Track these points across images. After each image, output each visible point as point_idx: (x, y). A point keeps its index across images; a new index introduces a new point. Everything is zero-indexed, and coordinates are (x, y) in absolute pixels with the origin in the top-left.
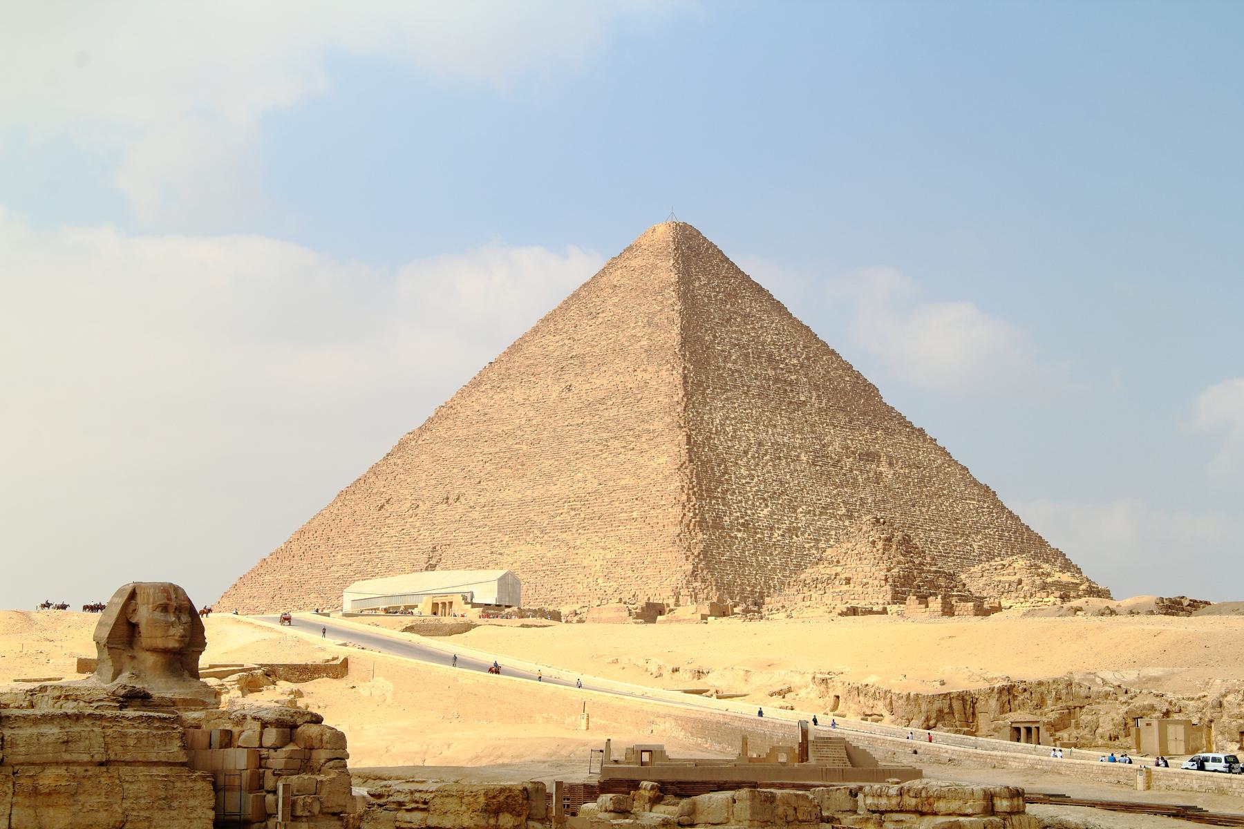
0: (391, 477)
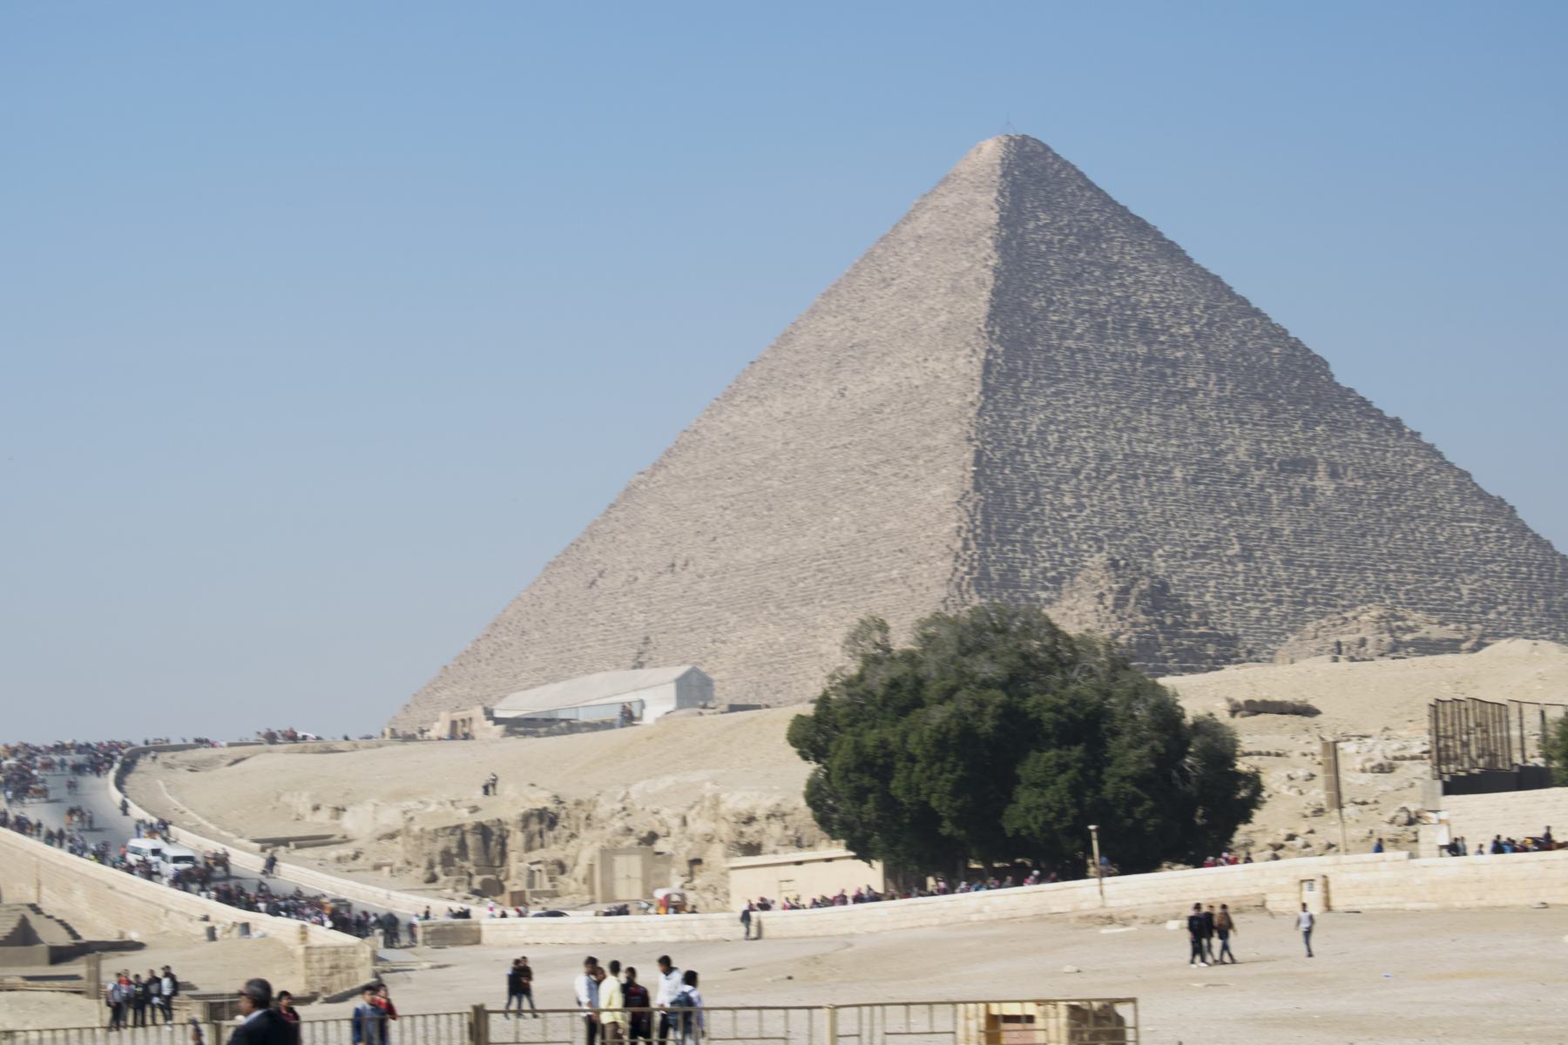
0: (609, 538)
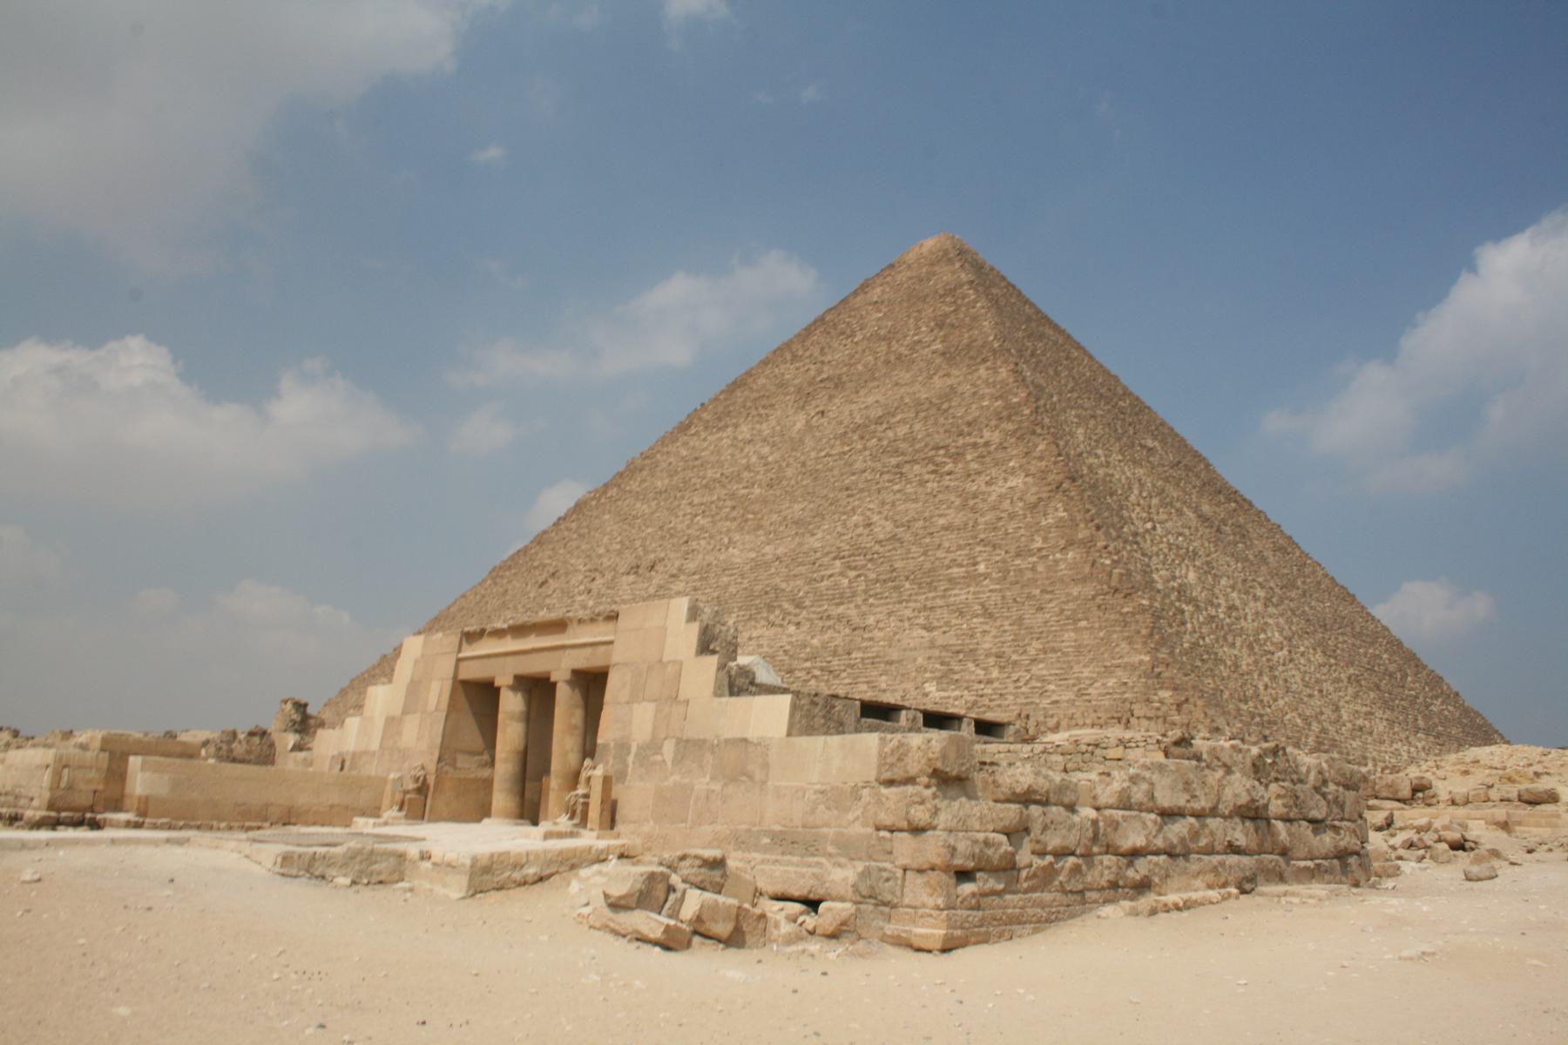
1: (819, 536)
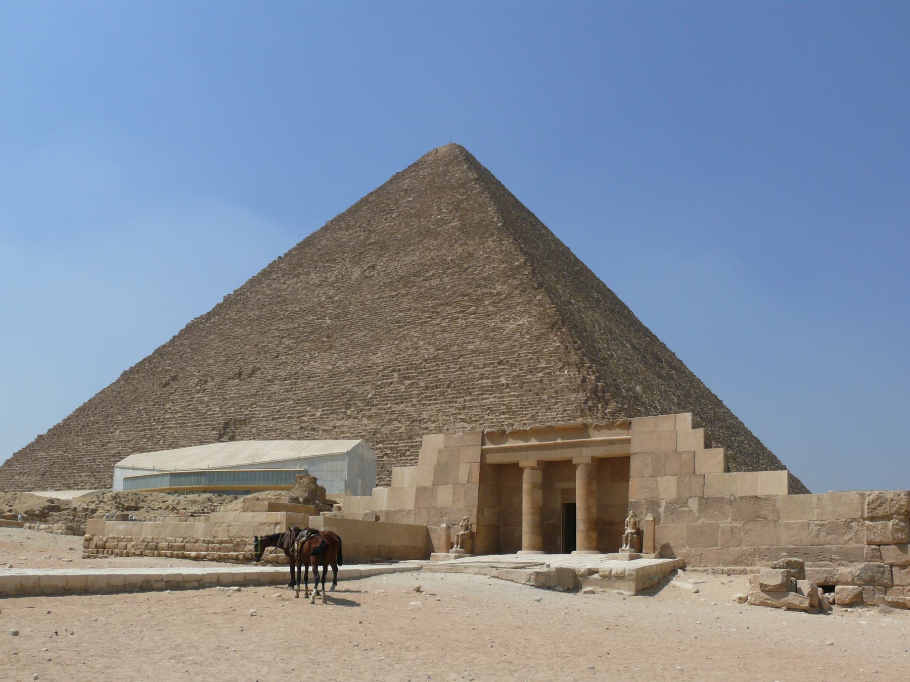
0: (178, 356)
1: (379, 355)
